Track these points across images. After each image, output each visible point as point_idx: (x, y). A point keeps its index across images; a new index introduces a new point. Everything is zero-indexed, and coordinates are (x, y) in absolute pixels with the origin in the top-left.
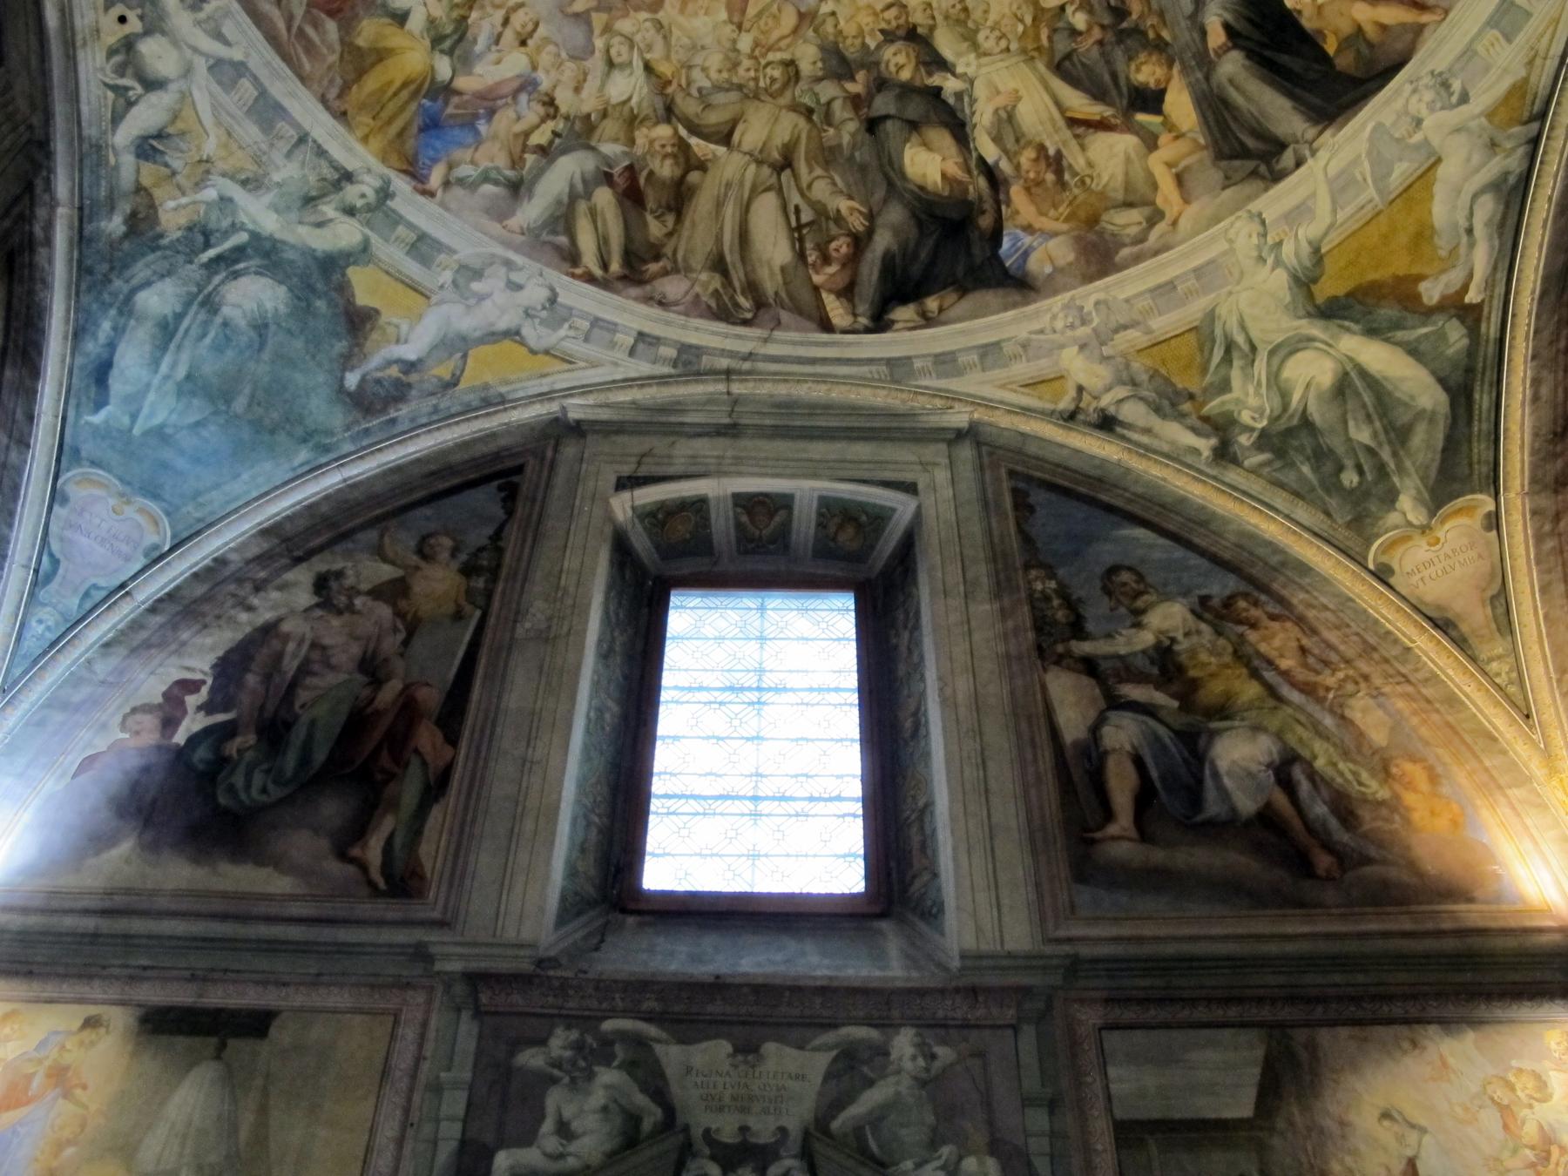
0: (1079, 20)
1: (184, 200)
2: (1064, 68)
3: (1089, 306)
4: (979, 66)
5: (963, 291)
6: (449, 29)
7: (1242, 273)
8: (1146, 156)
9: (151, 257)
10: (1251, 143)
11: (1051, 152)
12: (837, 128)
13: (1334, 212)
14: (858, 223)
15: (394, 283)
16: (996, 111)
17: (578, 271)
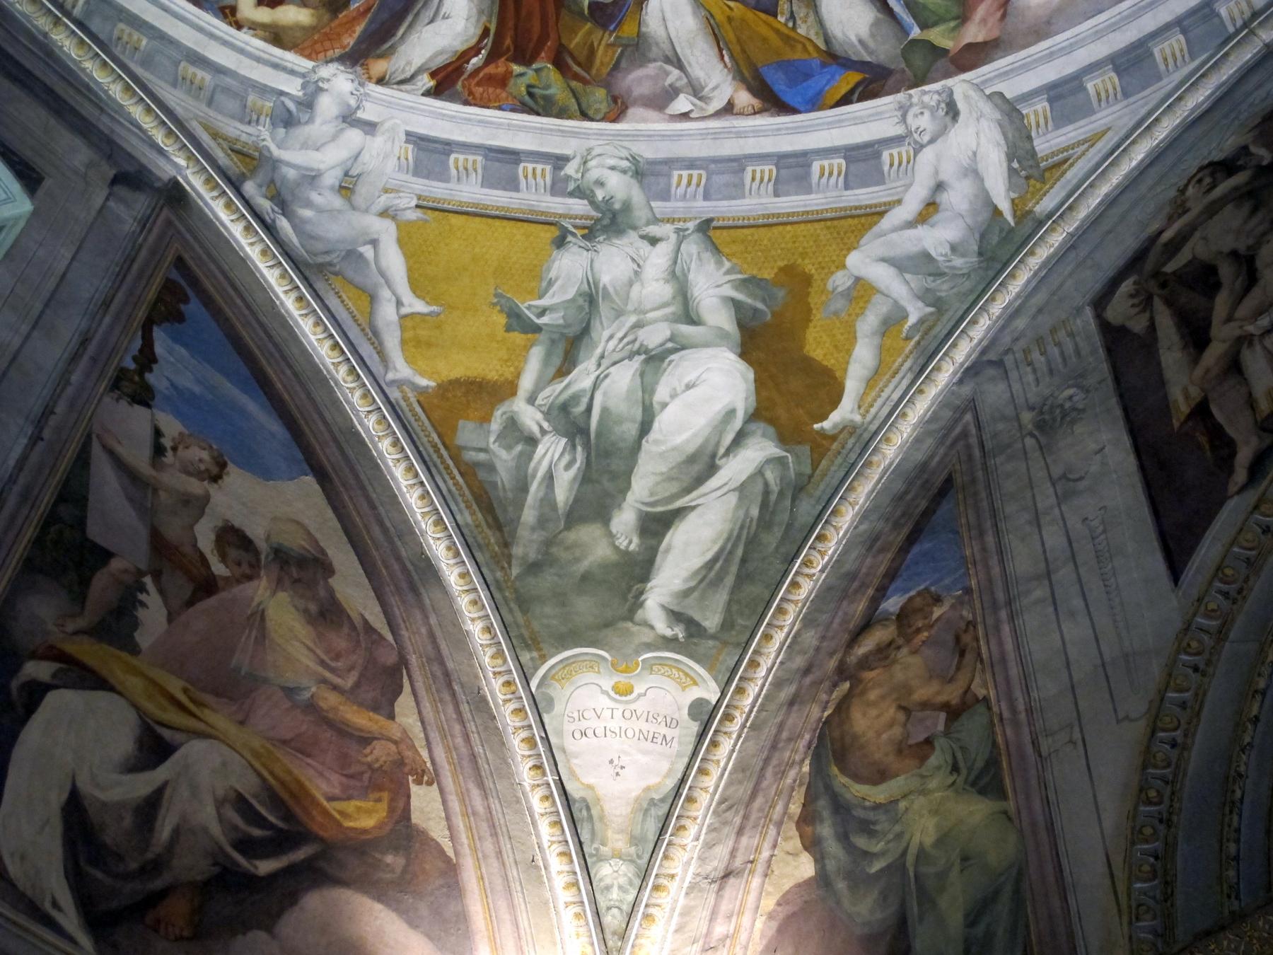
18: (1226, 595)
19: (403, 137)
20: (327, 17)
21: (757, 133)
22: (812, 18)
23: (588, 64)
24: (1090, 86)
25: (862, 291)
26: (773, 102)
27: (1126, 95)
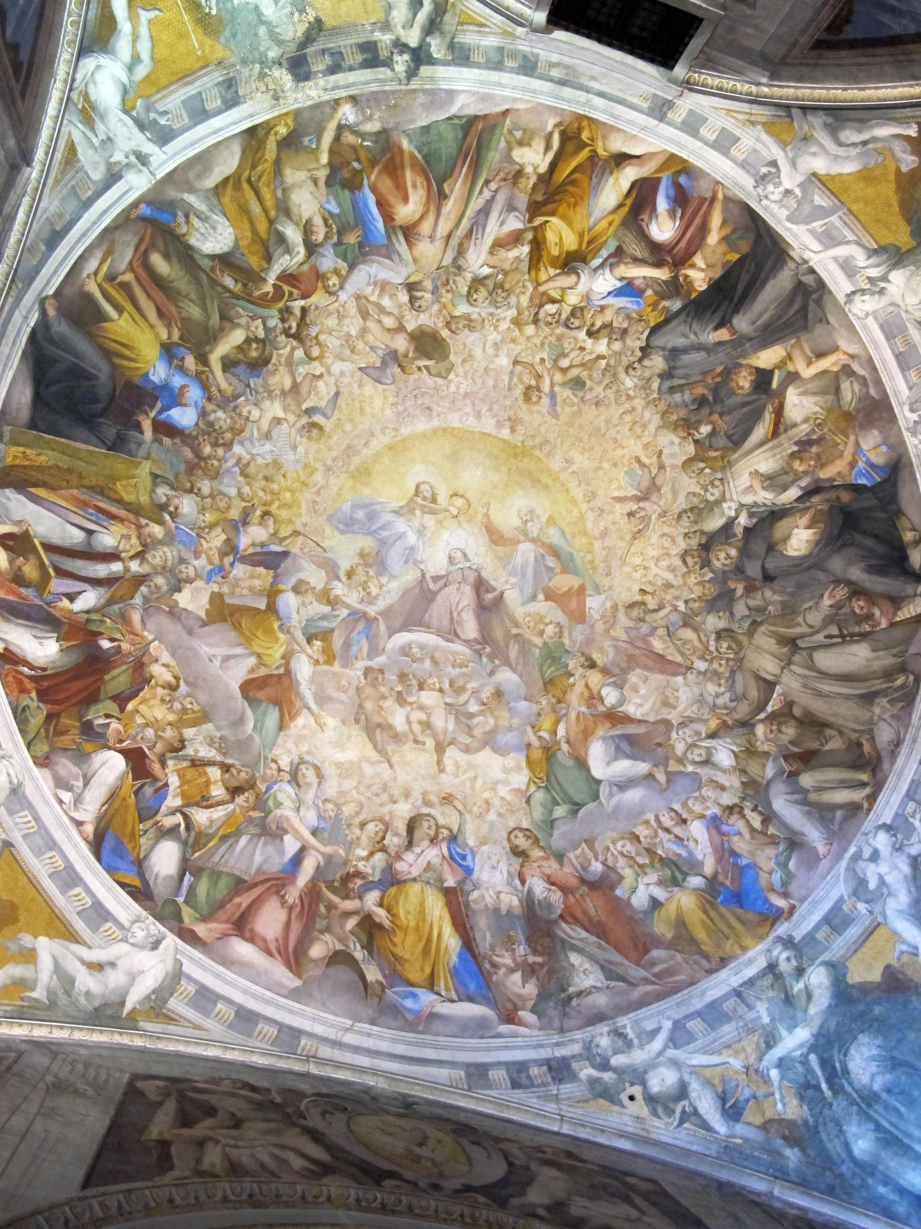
0: (705, 429)
1: (777, 1096)
2: (737, 439)
3: (914, 417)
4: (732, 500)
5: (899, 512)
6: (668, 872)
7: (893, 304)
8: (803, 380)
9: (824, 1136)
10: (796, 306)
11: (796, 448)
12: (768, 604)
13: (848, 242)
14: (841, 593)
15: (864, 949)
16: (764, 488)
17: (866, 805)
18: (120, 1206)
21: (75, 846)
24: (219, 1006)
25: (29, 956)
26: (97, 845)
27: (230, 1026)
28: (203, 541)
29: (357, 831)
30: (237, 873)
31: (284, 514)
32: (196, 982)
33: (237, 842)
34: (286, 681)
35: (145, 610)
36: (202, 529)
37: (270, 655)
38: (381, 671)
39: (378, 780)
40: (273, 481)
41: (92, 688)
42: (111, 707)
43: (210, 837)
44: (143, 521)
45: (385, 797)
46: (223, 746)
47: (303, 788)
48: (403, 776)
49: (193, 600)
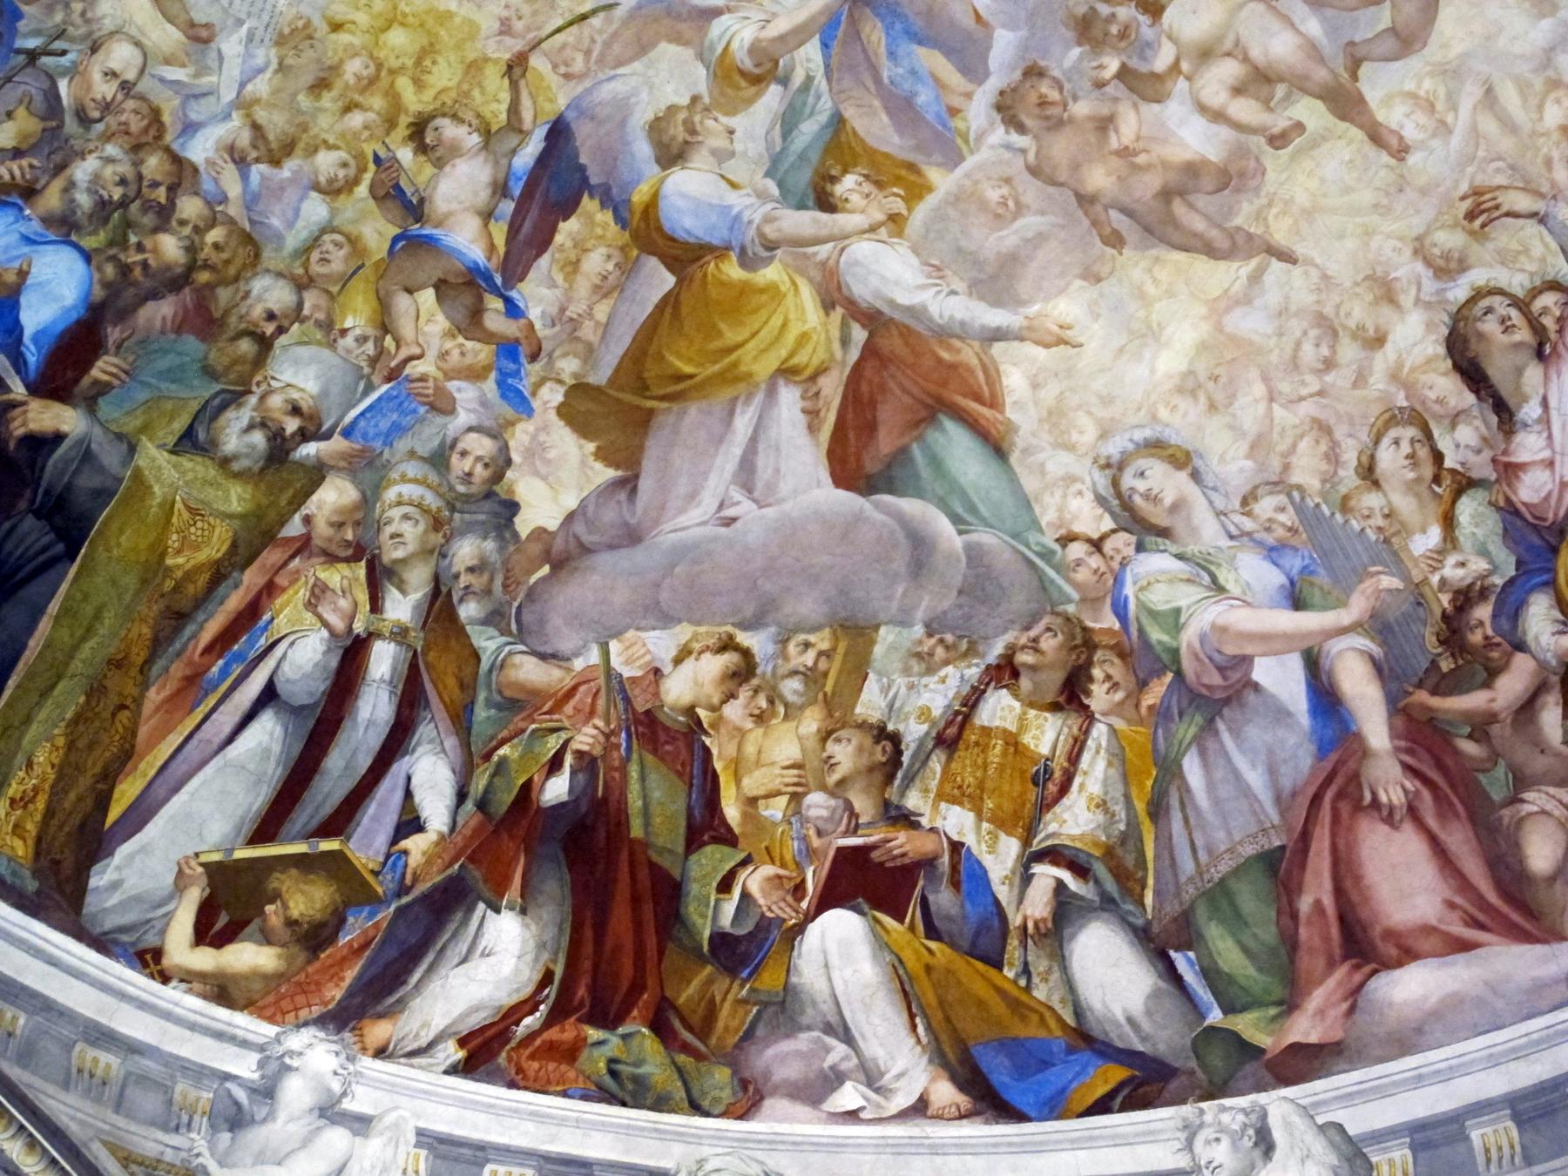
19: (412, 1139)
20: (302, 957)
22: (1056, 975)
23: (705, 1028)
24: (1475, 1135)
27: (1529, 1161)
28: (415, 369)
29: (1372, 500)
30: (1249, 850)
31: (444, 76)
32: (1392, 1133)
33: (1185, 789)
34: (891, 343)
35: (522, 635)
36: (373, 361)
37: (804, 338)
38: (1034, 72)
39: (1296, 327)
40: (336, 69)
41: (643, 875)
42: (711, 861)
43: (1132, 837)
44: (294, 528)
45: (1349, 352)
46: (949, 637)
47: (1179, 527)
48: (1337, 254)
49: (555, 480)
